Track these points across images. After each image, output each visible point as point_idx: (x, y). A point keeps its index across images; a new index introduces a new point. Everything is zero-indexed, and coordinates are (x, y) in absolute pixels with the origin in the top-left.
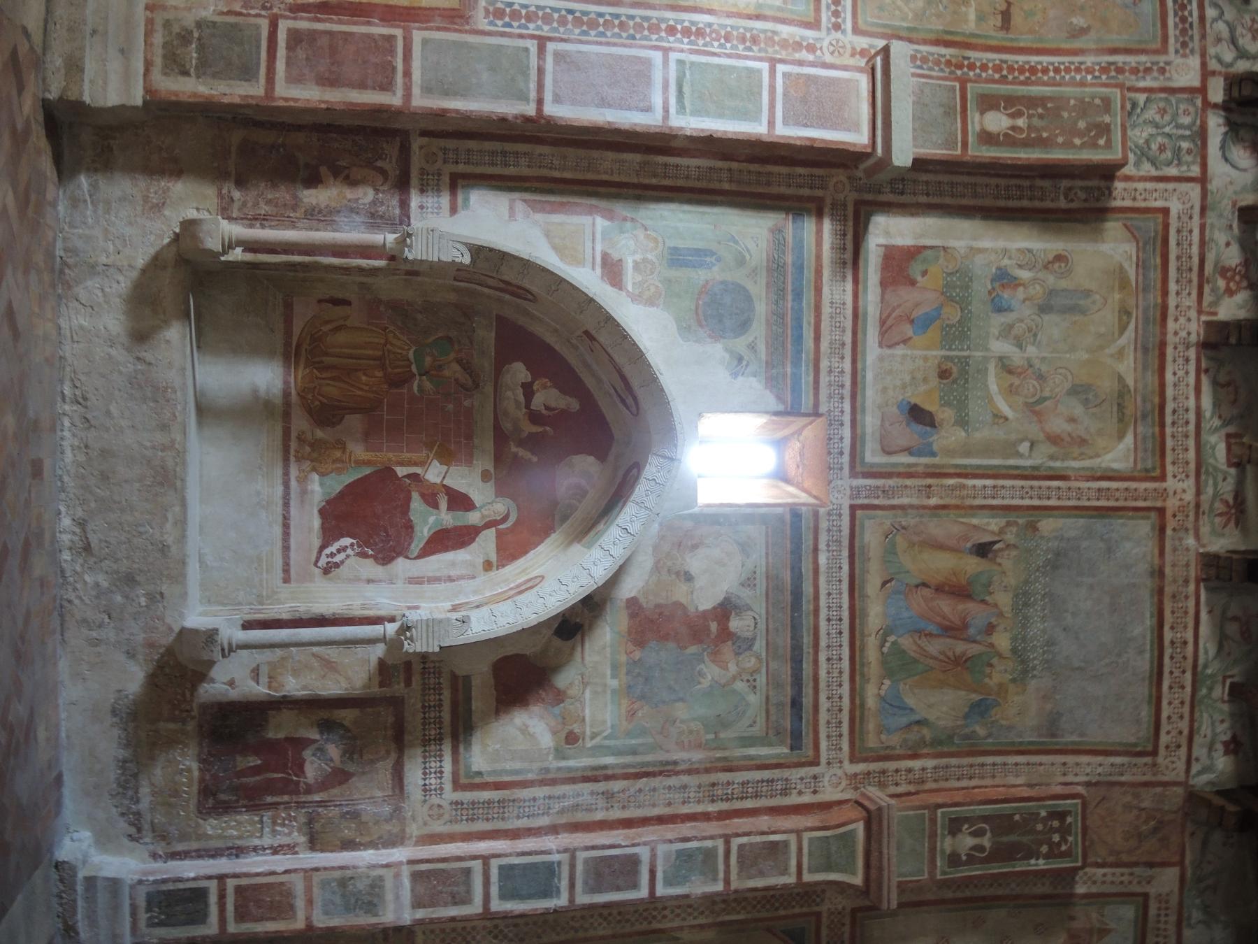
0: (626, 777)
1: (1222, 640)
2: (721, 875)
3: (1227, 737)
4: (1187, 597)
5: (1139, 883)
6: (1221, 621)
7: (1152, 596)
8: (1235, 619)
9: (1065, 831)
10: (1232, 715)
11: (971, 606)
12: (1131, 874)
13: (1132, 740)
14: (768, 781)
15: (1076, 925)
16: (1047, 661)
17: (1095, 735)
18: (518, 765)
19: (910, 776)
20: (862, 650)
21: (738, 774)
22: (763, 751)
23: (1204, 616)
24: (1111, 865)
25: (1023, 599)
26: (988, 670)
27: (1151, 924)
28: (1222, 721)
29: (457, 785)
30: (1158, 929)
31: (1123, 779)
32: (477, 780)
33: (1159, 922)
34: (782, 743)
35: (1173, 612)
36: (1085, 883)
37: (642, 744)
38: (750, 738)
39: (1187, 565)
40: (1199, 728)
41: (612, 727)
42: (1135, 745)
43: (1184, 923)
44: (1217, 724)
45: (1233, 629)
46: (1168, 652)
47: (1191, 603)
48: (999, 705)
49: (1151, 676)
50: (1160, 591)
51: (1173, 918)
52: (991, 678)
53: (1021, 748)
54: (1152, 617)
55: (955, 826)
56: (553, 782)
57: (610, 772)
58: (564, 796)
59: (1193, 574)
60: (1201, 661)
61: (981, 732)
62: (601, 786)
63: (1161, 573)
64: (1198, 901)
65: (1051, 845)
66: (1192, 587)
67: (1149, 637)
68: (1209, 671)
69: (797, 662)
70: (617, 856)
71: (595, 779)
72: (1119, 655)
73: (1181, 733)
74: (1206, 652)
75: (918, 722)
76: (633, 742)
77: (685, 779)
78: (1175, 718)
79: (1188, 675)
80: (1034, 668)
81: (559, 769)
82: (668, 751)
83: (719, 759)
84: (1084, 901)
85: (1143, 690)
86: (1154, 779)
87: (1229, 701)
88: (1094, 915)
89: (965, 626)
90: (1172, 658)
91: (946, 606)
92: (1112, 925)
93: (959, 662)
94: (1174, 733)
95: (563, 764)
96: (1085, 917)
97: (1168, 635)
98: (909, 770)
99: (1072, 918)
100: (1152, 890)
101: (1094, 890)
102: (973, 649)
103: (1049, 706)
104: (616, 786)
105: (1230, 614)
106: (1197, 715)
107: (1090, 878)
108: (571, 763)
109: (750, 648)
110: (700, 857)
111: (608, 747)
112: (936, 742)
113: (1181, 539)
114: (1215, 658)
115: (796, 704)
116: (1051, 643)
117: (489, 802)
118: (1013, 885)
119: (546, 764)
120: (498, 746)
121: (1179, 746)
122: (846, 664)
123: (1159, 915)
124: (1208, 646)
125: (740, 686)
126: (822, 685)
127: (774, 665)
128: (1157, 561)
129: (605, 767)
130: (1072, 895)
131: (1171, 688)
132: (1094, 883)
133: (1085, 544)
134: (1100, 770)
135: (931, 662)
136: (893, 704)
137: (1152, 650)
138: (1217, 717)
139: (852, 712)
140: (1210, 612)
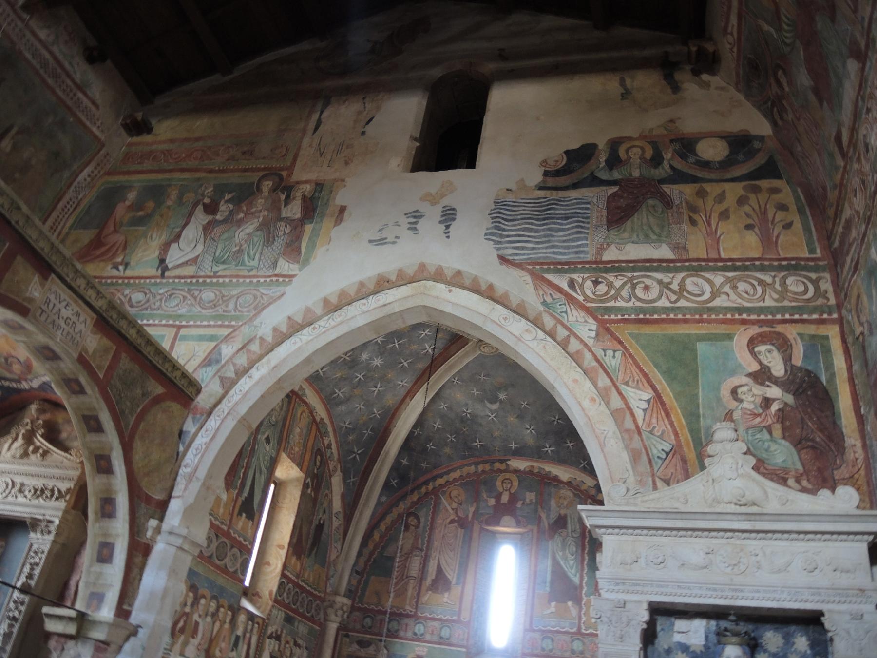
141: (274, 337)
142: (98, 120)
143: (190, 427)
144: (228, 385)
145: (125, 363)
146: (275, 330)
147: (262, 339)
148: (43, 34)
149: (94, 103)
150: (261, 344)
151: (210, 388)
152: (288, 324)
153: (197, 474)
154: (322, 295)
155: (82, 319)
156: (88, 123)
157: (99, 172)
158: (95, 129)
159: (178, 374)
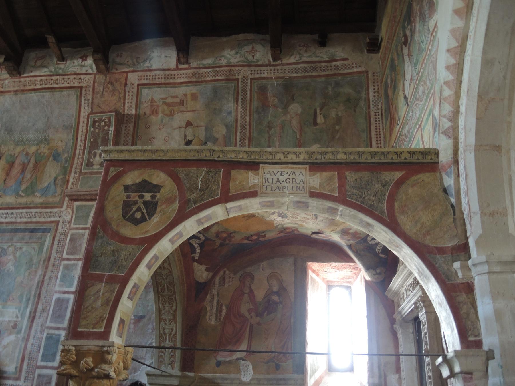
0: (38, 303)
1: (43, 66)
2: (76, 262)
3: (80, 60)
4: (25, 81)
5: (133, 89)
6: (36, 67)
7: (24, 94)
8: (35, 63)
9: (101, 120)
10: (71, 60)
11: (17, 161)
12: (129, 92)
13: (75, 97)
14: (59, 242)
15: (148, 112)
16: (43, 132)
17: (73, 111)
18: (17, 351)
19: (74, 183)
20: (21, 204)
21: (52, 255)
22: (47, 243)
23: (32, 74)
24: (125, 100)
25: (21, 142)
26: (42, 154)
27: (151, 82)
28: (74, 63)
29: (18, 379)
30: (152, 79)
31: (90, 99)
32: (18, 369)
33: (149, 79)
34: (46, 236)
35: (30, 86)
36: (131, 110)
37: (26, 296)
38: (39, 250)
39: (14, 82)
40: (74, 72)
41: (16, 308)
42: (77, 95)
43: (150, 68)
44: (74, 65)
45: (39, 63)
46: (44, 86)
47: (28, 79)
48: (56, 149)
49: (52, 92)
50: (23, 91)
51: (148, 73)
52: (45, 153)
53: (75, 139)
54: (30, 93)
55: (90, 164)
56: (29, 335)
57: (33, 310)
58: (36, 331)
59: (18, 80)
60: (49, 73)
61: (66, 155)
62: (38, 314)
63: (16, 92)
64: (142, 64)
65: (105, 125)
66: (22, 80)
67: (39, 94)
68: (53, 70)
69: (16, 231)
70: (54, 308)
71: (34, 317)
72: (44, 104)
73: (74, 78)
74: (46, 72)
75: (55, 181)
76: (24, 300)
77: (47, 278)
78: (69, 81)
79: (53, 78)
80: (45, 136)
81: (25, 332)
82: (33, 285)
83: (44, 263)
84: (138, 110)
85: (57, 94)
86: (92, 87)
87: (66, 61)
88: (145, 105)
89: (24, 164)
90: (46, 85)
91: (16, 170)
92: (150, 97)
93: (36, 166)
94: (74, 81)
95: (23, 331)
96: (145, 108)
97: (39, 87)
98: (73, 183)
99: (145, 114)
100: (137, 83)
101: (134, 106)
102: (33, 161)
103: (60, 130)
104: (40, 307)
105: (34, 65)
106: (69, 73)
107: (129, 108)
108: (24, 327)
109: (5, 250)
110: (66, 271)
111: (23, 311)
112: (65, 174)
113: (6, 85)
114: (48, 68)
115: (33, 231)
116: (37, 130)
117: (28, 364)
118: (128, 139)
119: (21, 338)
120: (8, 359)
121: (80, 78)
122: (24, 211)
123: (147, 79)
124: (45, 71)
125: (18, 254)
126: (29, 220)
127: (15, 239)
128: (12, 93)
129: (30, 312)
130: (136, 115)
131: (57, 84)
132: (131, 106)
133: (4, 120)
134: (86, 108)
135: (34, 177)
136: (45, 192)
137: (43, 92)
138: (72, 65)
139: (42, 208)
140: (32, 72)
141: (452, 73)
142: (353, 64)
143: (449, 181)
144: (453, 133)
145: (351, 176)
146: (448, 68)
147: (446, 83)
148: (292, 60)
149: (343, 60)
150: (449, 87)
151: (444, 146)
152: (451, 55)
153: (472, 210)
154: (450, 11)
155: (297, 174)
156: (350, 71)
157: (378, 86)
158: (355, 70)
159: (408, 156)
